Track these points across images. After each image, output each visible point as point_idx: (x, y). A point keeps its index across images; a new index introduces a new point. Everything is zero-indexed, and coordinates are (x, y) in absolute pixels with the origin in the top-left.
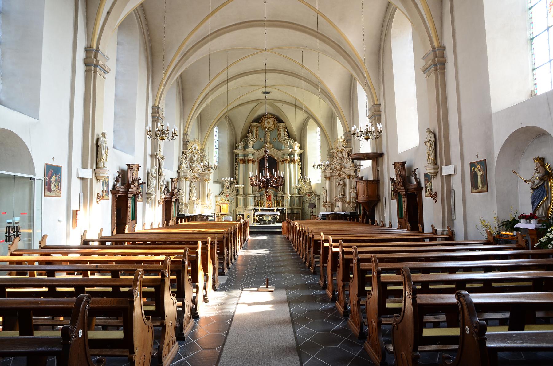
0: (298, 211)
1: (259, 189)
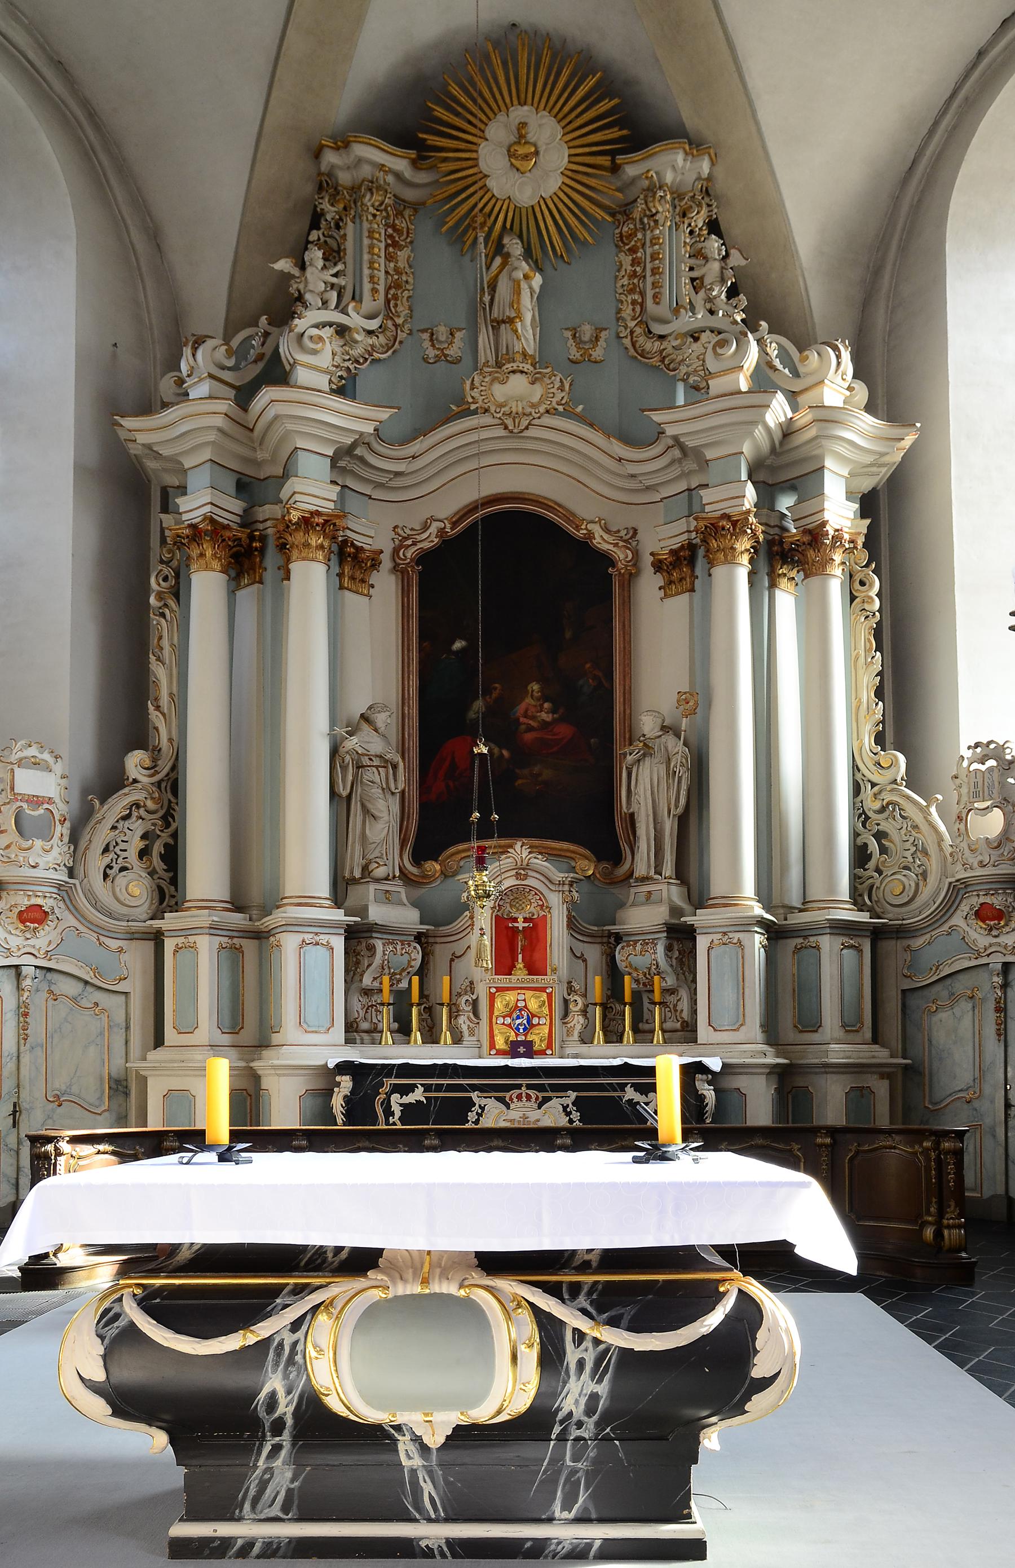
0: (858, 1098)
1: (418, 858)
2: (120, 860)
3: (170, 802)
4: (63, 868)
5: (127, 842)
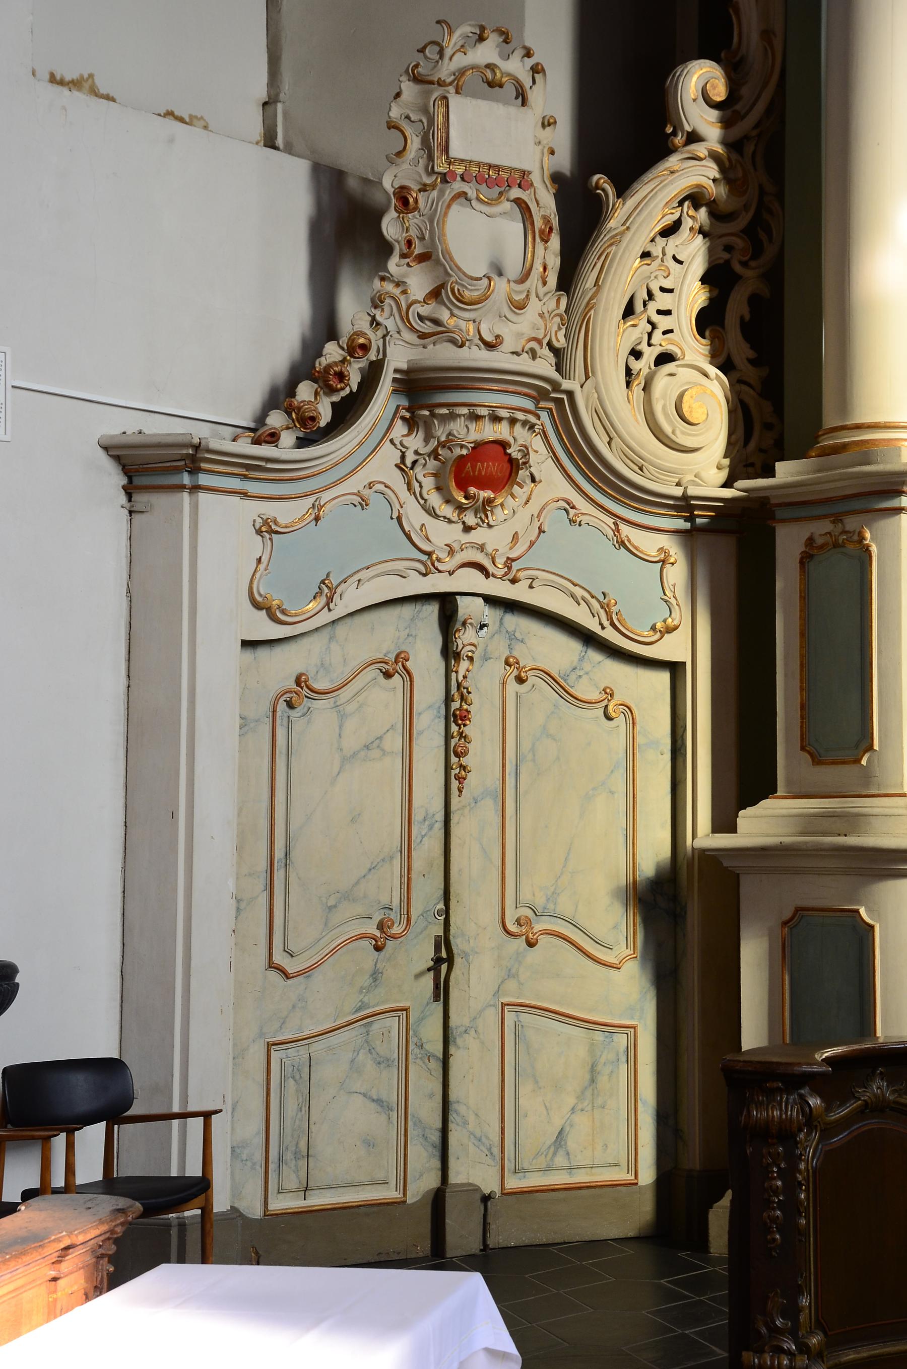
2: (657, 337)
3: (762, 191)
4: (546, 351)
5: (671, 291)
